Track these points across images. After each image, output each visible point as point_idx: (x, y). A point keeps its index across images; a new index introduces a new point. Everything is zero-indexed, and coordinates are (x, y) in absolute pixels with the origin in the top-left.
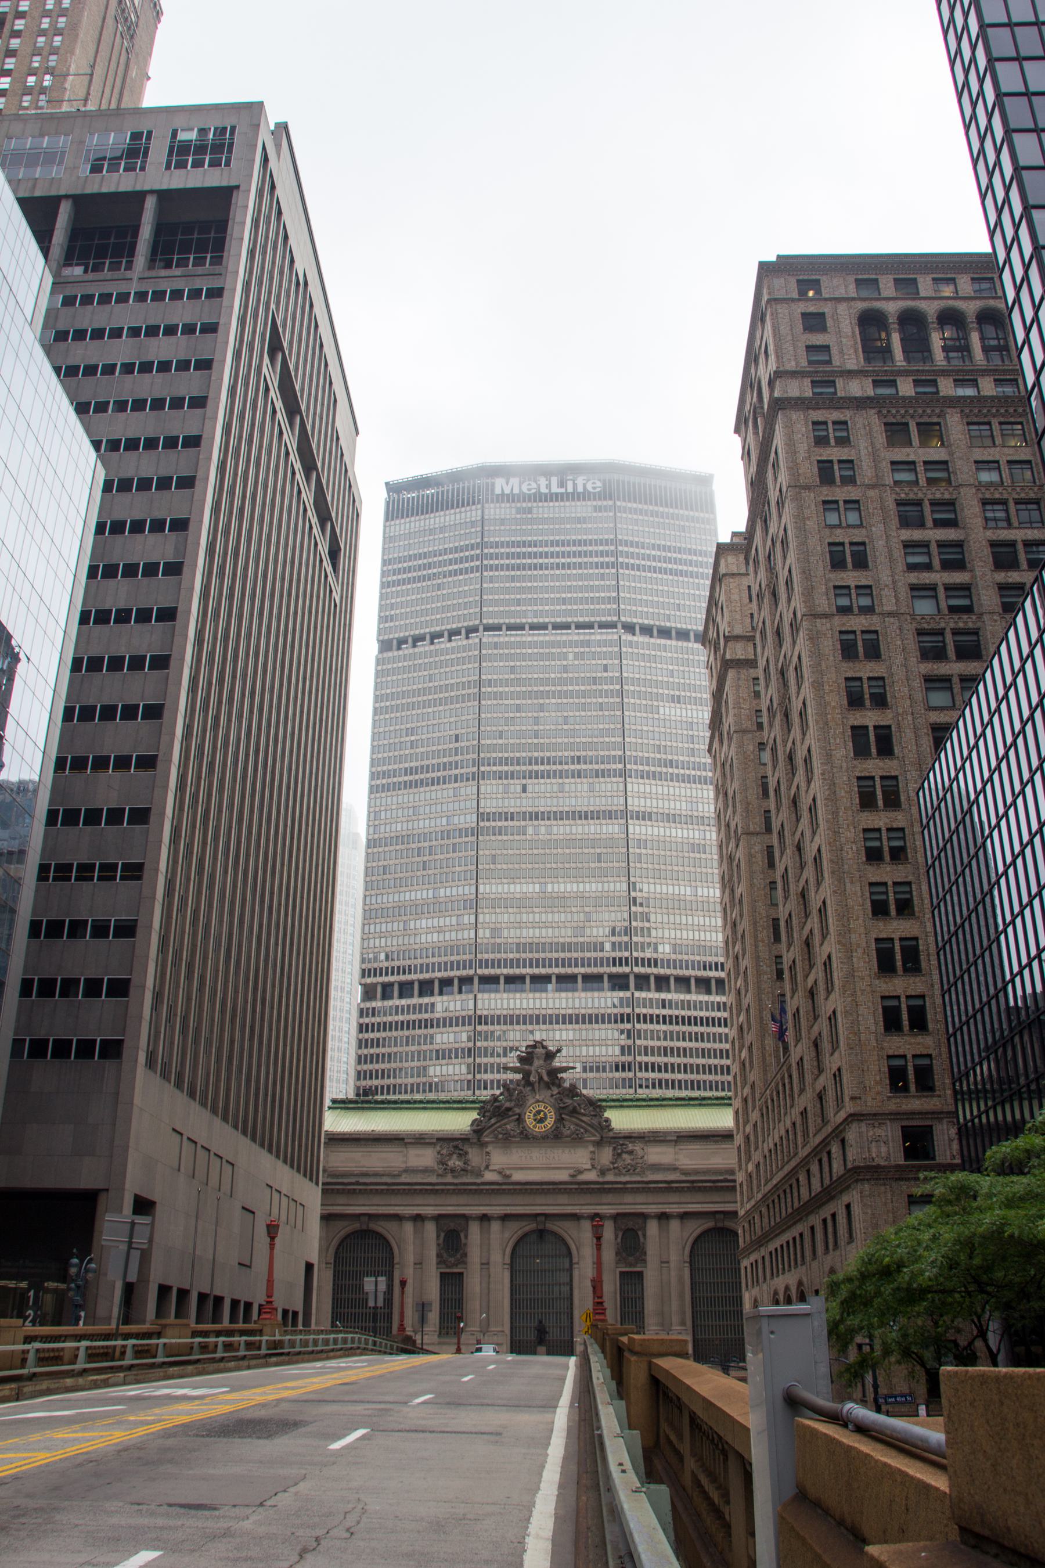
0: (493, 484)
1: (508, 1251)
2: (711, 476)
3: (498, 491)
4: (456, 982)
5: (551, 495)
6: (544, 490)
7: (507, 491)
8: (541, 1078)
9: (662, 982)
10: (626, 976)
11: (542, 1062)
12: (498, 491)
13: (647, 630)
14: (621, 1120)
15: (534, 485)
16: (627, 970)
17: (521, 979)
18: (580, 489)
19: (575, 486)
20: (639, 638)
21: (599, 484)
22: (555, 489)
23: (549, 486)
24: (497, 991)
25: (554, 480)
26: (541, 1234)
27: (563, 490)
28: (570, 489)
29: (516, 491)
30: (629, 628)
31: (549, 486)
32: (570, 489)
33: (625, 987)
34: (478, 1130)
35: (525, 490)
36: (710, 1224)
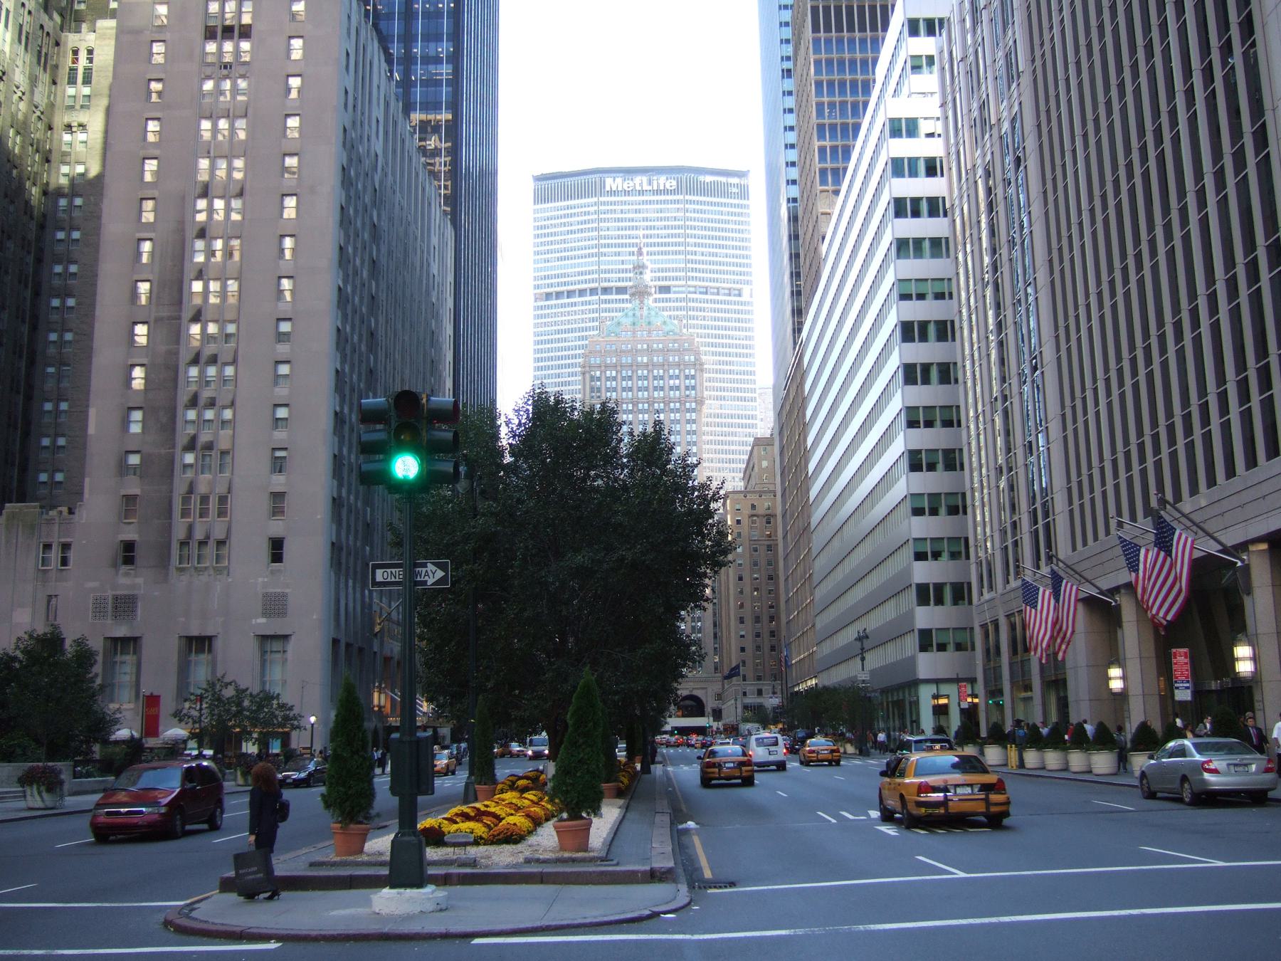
3: (608, 188)
6: (638, 188)
12: (608, 188)
15: (631, 184)
21: (674, 183)
22: (646, 187)
23: (641, 184)
31: (641, 184)
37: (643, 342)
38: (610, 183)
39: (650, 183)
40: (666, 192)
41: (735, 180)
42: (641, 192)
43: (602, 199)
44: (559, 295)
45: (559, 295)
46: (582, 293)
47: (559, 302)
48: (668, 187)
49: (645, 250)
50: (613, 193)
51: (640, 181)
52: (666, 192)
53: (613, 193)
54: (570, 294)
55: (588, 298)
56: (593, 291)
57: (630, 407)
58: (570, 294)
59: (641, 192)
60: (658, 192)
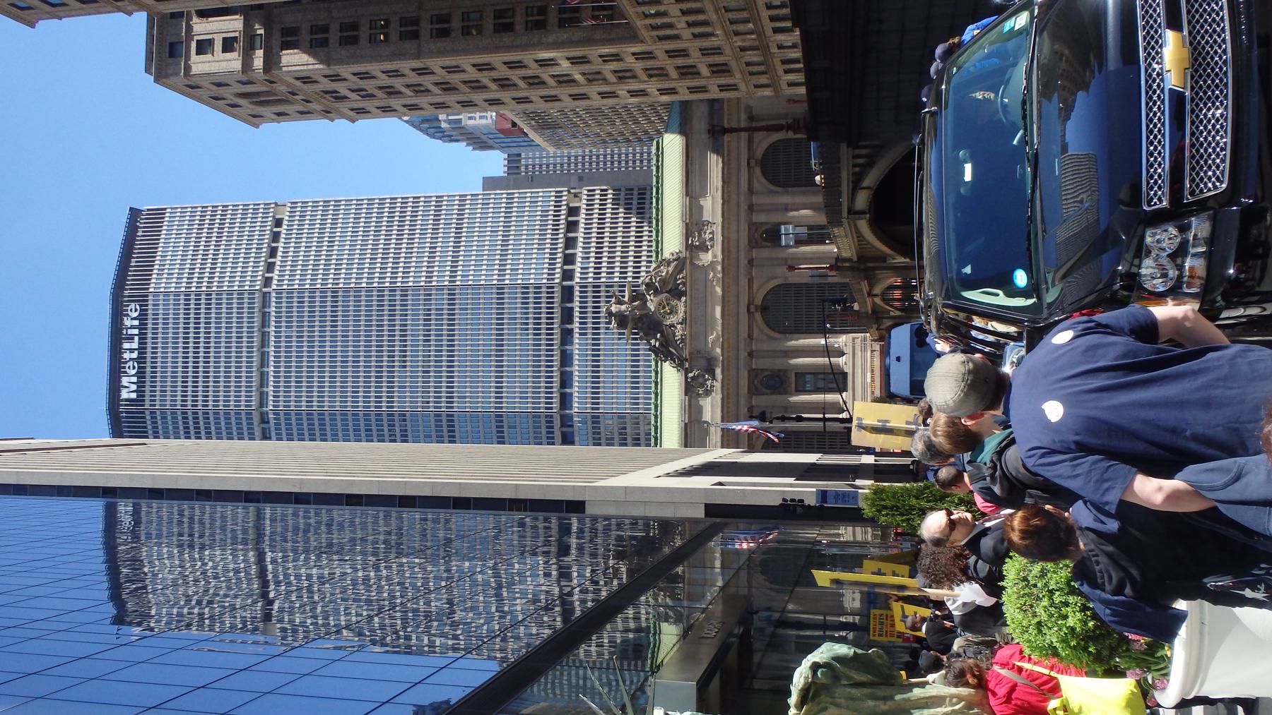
0: (126, 400)
1: (777, 335)
2: (131, 209)
4: (565, 429)
5: (139, 348)
6: (135, 355)
8: (636, 308)
9: (569, 259)
10: (563, 288)
11: (623, 307)
12: (134, 396)
13: (270, 267)
14: (672, 242)
16: (557, 289)
17: (562, 374)
18: (136, 323)
19: (133, 327)
20: (275, 275)
21: (133, 306)
22: (135, 345)
23: (131, 351)
24: (571, 394)
25: (126, 346)
26: (764, 309)
28: (136, 331)
29: (134, 379)
30: (267, 282)
31: (131, 351)
32: (136, 331)
33: (571, 288)
34: (680, 364)
35: (133, 372)
36: (758, 170)
39: (131, 338)
48: (135, 315)
51: (130, 349)
52: (142, 317)
53: (140, 391)
59: (142, 349)
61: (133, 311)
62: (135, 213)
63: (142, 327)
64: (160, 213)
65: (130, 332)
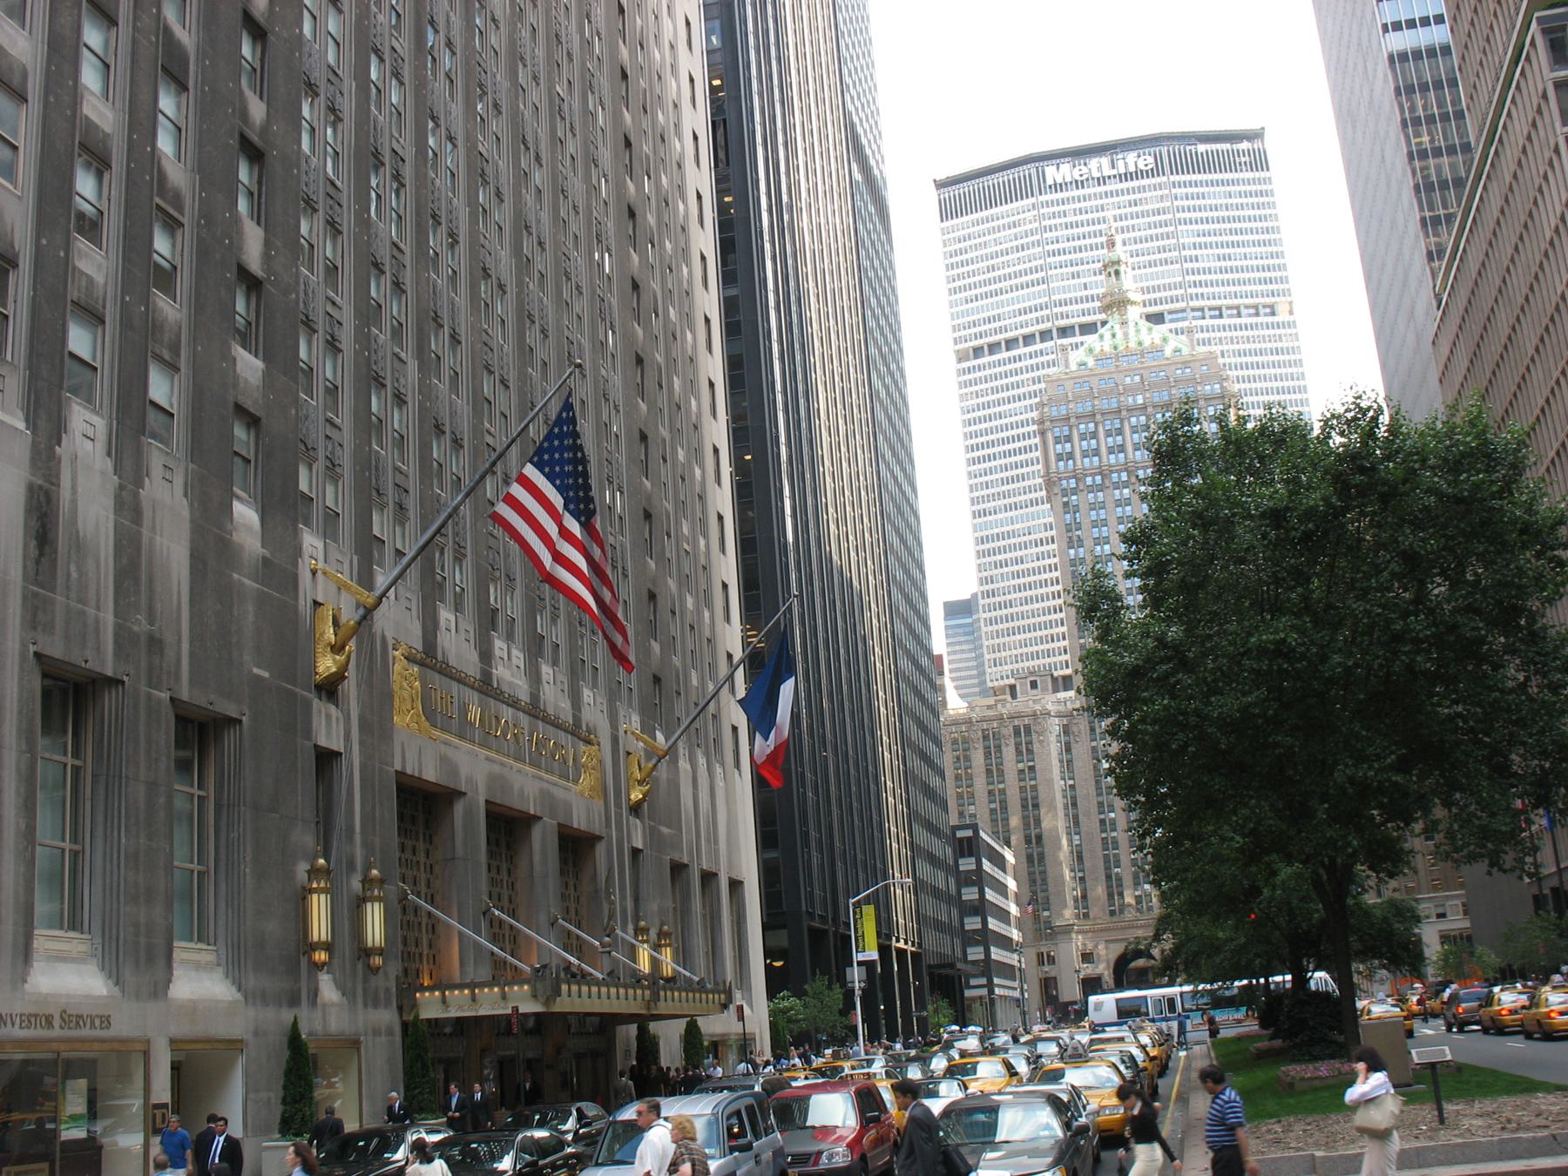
3: (1050, 181)
6: (1096, 174)
7: (1059, 180)
12: (1050, 181)
15: (1085, 170)
21: (1151, 160)
22: (1107, 172)
23: (1100, 168)
27: (1114, 172)
28: (1122, 171)
29: (1068, 179)
31: (1100, 168)
37: (1129, 372)
38: (1052, 173)
40: (1139, 174)
41: (1245, 145)
42: (1102, 180)
43: (1043, 198)
44: (993, 348)
45: (993, 348)
46: (1028, 339)
47: (995, 357)
48: (1141, 166)
49: (1118, 239)
50: (1057, 187)
52: (1139, 174)
53: (1057, 187)
54: (1011, 344)
55: (1038, 346)
56: (1045, 335)
57: (1124, 477)
58: (1011, 344)
59: (1102, 180)
60: (1127, 176)
61: (1146, 161)
62: (1255, 136)
63: (1127, 176)
64: (1259, 162)
65: (1121, 164)
